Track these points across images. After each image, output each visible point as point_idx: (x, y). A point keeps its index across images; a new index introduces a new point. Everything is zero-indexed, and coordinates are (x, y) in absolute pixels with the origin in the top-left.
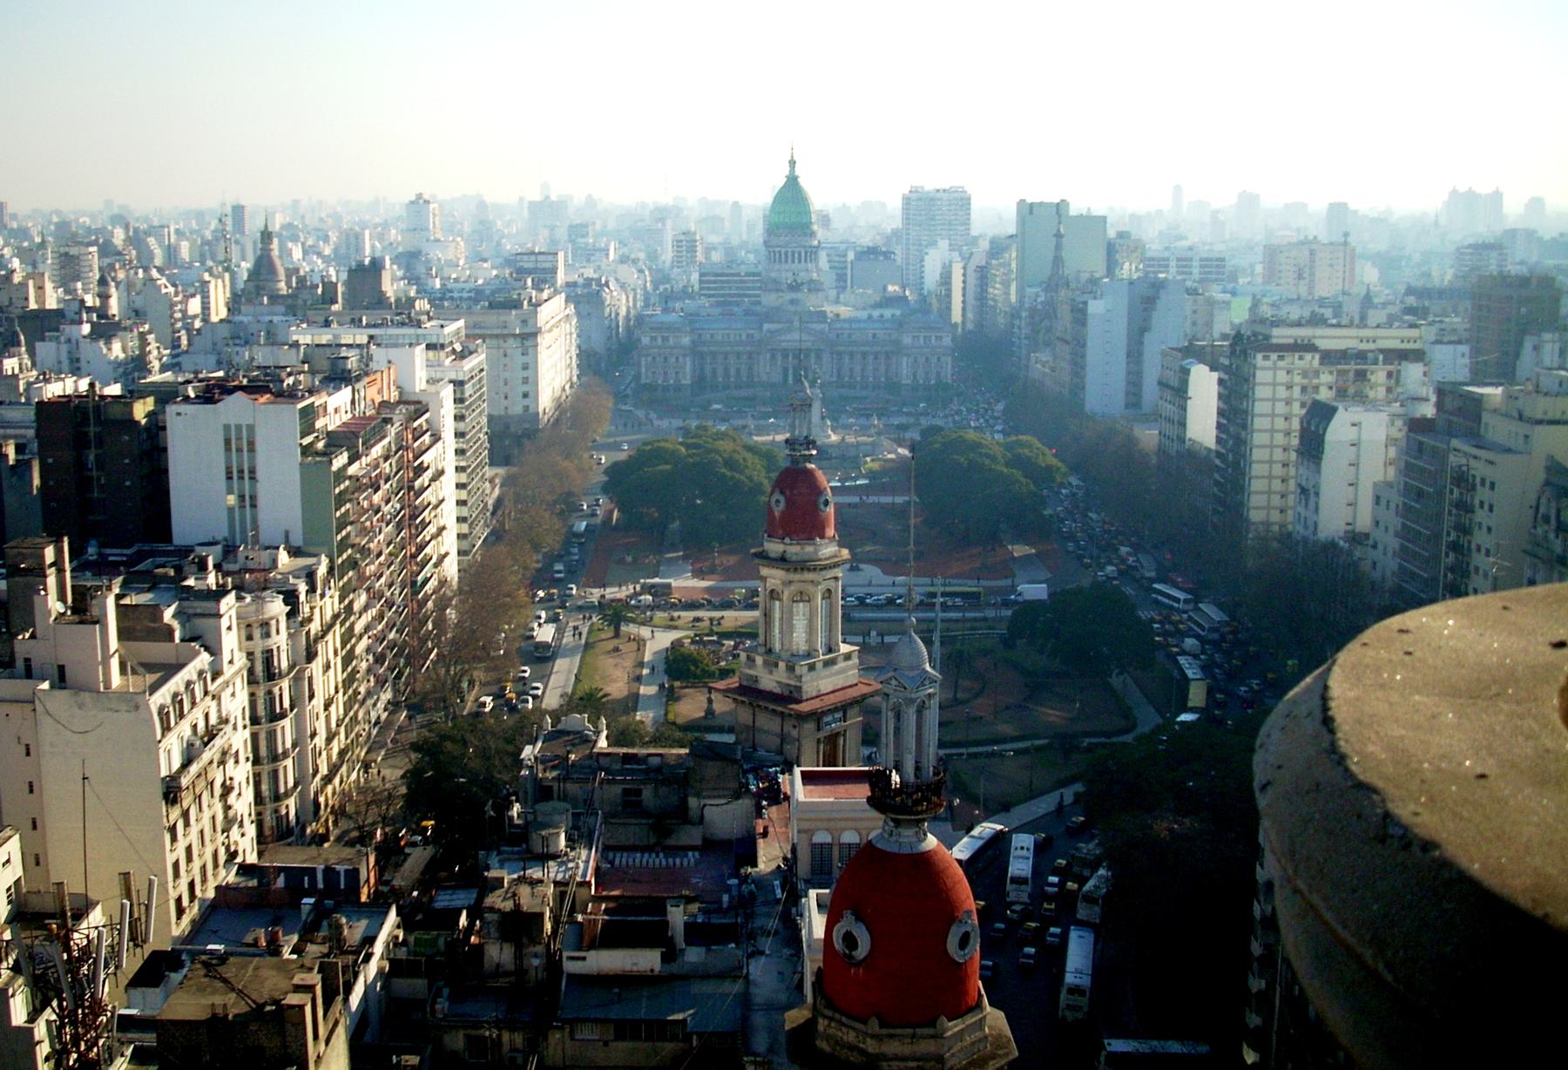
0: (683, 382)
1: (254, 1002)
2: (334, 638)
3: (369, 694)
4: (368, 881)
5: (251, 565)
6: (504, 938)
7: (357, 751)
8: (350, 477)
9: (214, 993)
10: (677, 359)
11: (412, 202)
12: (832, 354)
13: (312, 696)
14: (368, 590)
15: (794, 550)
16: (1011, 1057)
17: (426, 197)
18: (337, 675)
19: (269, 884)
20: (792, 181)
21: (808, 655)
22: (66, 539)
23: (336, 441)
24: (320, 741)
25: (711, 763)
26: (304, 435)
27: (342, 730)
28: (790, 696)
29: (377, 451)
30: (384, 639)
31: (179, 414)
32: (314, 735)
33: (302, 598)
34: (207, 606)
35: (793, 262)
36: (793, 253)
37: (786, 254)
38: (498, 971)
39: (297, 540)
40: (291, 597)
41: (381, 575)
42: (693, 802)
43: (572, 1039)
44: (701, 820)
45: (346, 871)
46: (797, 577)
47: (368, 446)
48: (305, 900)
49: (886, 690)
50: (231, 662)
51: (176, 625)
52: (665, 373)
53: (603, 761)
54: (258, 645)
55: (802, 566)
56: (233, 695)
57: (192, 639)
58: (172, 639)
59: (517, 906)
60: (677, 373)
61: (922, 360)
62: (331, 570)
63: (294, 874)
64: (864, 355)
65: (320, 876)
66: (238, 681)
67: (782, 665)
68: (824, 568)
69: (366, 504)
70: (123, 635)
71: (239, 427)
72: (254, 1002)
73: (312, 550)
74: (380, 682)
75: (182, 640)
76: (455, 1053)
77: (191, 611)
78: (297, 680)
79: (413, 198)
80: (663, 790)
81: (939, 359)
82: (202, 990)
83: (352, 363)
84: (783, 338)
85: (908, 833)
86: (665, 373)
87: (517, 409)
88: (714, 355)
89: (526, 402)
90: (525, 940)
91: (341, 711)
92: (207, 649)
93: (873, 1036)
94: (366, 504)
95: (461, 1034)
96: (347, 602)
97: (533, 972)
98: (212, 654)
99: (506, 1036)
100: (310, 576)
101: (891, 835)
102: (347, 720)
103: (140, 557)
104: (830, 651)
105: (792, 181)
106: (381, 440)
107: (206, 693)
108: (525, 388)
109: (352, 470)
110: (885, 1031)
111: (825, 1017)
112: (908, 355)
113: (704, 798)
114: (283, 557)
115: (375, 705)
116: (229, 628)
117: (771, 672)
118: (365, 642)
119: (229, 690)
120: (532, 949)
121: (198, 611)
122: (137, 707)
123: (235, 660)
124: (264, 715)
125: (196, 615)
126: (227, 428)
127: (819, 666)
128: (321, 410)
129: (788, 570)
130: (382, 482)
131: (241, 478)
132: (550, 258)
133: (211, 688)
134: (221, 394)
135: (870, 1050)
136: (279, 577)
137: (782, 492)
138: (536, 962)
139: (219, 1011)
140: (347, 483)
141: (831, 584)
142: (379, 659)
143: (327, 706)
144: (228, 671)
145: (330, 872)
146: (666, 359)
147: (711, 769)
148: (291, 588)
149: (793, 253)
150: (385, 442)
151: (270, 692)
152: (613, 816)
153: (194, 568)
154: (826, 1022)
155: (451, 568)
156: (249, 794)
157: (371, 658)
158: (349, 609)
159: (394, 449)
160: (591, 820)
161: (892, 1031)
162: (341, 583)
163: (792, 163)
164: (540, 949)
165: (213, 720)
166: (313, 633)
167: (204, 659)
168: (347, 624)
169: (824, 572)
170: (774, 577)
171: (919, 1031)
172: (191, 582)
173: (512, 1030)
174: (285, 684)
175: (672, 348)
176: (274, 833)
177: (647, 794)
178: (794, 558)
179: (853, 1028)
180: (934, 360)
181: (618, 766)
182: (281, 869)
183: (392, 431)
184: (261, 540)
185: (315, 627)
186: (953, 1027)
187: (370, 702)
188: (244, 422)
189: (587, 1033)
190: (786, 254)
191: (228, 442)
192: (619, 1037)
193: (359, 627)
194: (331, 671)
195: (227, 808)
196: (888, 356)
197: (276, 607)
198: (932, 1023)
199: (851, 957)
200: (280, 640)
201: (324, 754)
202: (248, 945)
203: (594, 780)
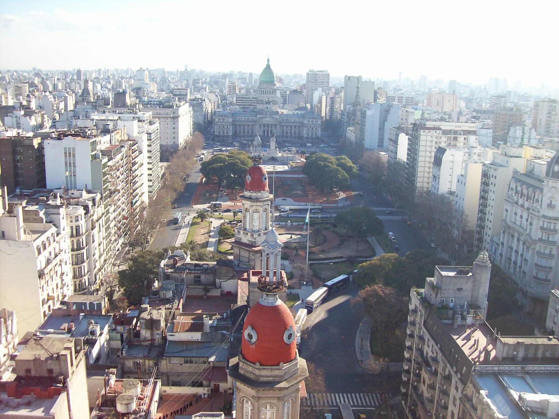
0: (230, 134)
1: (51, 353)
2: (102, 221)
3: (116, 240)
4: (105, 307)
5: (73, 196)
6: (147, 328)
7: (111, 260)
8: (109, 166)
9: (37, 349)
11: (138, 71)
12: (280, 126)
13: (93, 242)
14: (114, 205)
15: (254, 195)
16: (306, 376)
17: (144, 69)
18: (103, 234)
19: (70, 308)
20: (268, 67)
21: (259, 231)
22: (6, 187)
23: (105, 153)
24: (97, 257)
25: (224, 267)
26: (92, 151)
27: (105, 253)
28: (251, 245)
29: (119, 157)
30: (121, 221)
31: (49, 143)
32: (94, 255)
33: (90, 208)
34: (55, 211)
37: (266, 91)
38: (145, 340)
39: (90, 187)
40: (86, 208)
41: (120, 200)
42: (217, 281)
43: (170, 363)
44: (220, 287)
45: (97, 304)
46: (254, 204)
47: (115, 155)
48: (81, 314)
49: (264, 249)
50: (64, 230)
51: (44, 217)
52: (223, 131)
53: (188, 266)
54: (74, 224)
55: (257, 200)
56: (65, 241)
57: (50, 222)
58: (42, 222)
59: (151, 317)
60: (227, 131)
61: (310, 129)
62: (101, 198)
63: (79, 305)
65: (88, 305)
66: (67, 237)
67: (249, 234)
68: (264, 201)
69: (115, 175)
70: (25, 220)
71: (69, 148)
72: (51, 353)
73: (95, 191)
74: (120, 236)
75: (46, 222)
76: (129, 368)
77: (50, 213)
78: (88, 237)
79: (139, 69)
80: (208, 276)
81: (316, 128)
82: (32, 349)
83: (111, 127)
84: (264, 120)
85: (271, 299)
86: (223, 131)
87: (172, 143)
88: (240, 125)
89: (174, 140)
90: (154, 329)
91: (105, 248)
92: (55, 225)
93: (257, 369)
94: (115, 175)
95: (131, 361)
96: (107, 209)
97: (157, 340)
98: (57, 227)
99: (147, 361)
100: (94, 200)
101: (265, 299)
102: (107, 249)
103: (35, 193)
104: (266, 229)
105: (268, 67)
106: (120, 153)
107: (54, 241)
109: (109, 164)
110: (262, 367)
111: (242, 362)
112: (306, 127)
113: (221, 279)
114: (84, 193)
115: (117, 244)
116: (63, 218)
117: (246, 237)
118: (114, 223)
119: (63, 239)
120: (157, 332)
121: (52, 212)
122: (29, 246)
123: (65, 229)
124: (77, 248)
125: (51, 214)
126: (65, 148)
127: (262, 234)
128: (99, 143)
129: (252, 202)
130: (120, 168)
131: (70, 166)
132: (185, 91)
133: (57, 239)
134: (63, 137)
135: (257, 374)
136: (83, 200)
137: (250, 175)
138: (158, 336)
139: (37, 356)
140: (107, 168)
141: (267, 207)
142: (119, 229)
143: (99, 245)
144: (63, 233)
145: (91, 304)
147: (224, 269)
148: (86, 204)
150: (122, 154)
151: (78, 240)
152: (191, 285)
153: (53, 197)
154: (242, 364)
155: (145, 199)
156: (71, 275)
157: (116, 228)
158: (108, 212)
159: (125, 156)
160: (182, 287)
161: (264, 367)
162: (105, 203)
163: (268, 60)
164: (159, 332)
165: (57, 251)
166: (94, 220)
167: (54, 229)
168: (107, 217)
169: (264, 203)
170: (248, 204)
171: (274, 367)
172: (50, 202)
173: (149, 360)
174: (84, 237)
175: (226, 123)
176: (80, 289)
177: (203, 277)
178: (254, 198)
179: (251, 366)
180: (315, 129)
181: (193, 268)
182: (74, 303)
183: (124, 150)
184: (77, 187)
185: (95, 218)
186: (286, 366)
187: (115, 243)
188: (72, 146)
189: (175, 361)
190: (266, 91)
191: (66, 153)
192: (186, 362)
193: (111, 218)
194: (101, 232)
195: (62, 280)
197: (81, 211)
198: (278, 365)
199: (250, 342)
200: (82, 223)
201: (98, 261)
202: (62, 329)
203: (184, 272)
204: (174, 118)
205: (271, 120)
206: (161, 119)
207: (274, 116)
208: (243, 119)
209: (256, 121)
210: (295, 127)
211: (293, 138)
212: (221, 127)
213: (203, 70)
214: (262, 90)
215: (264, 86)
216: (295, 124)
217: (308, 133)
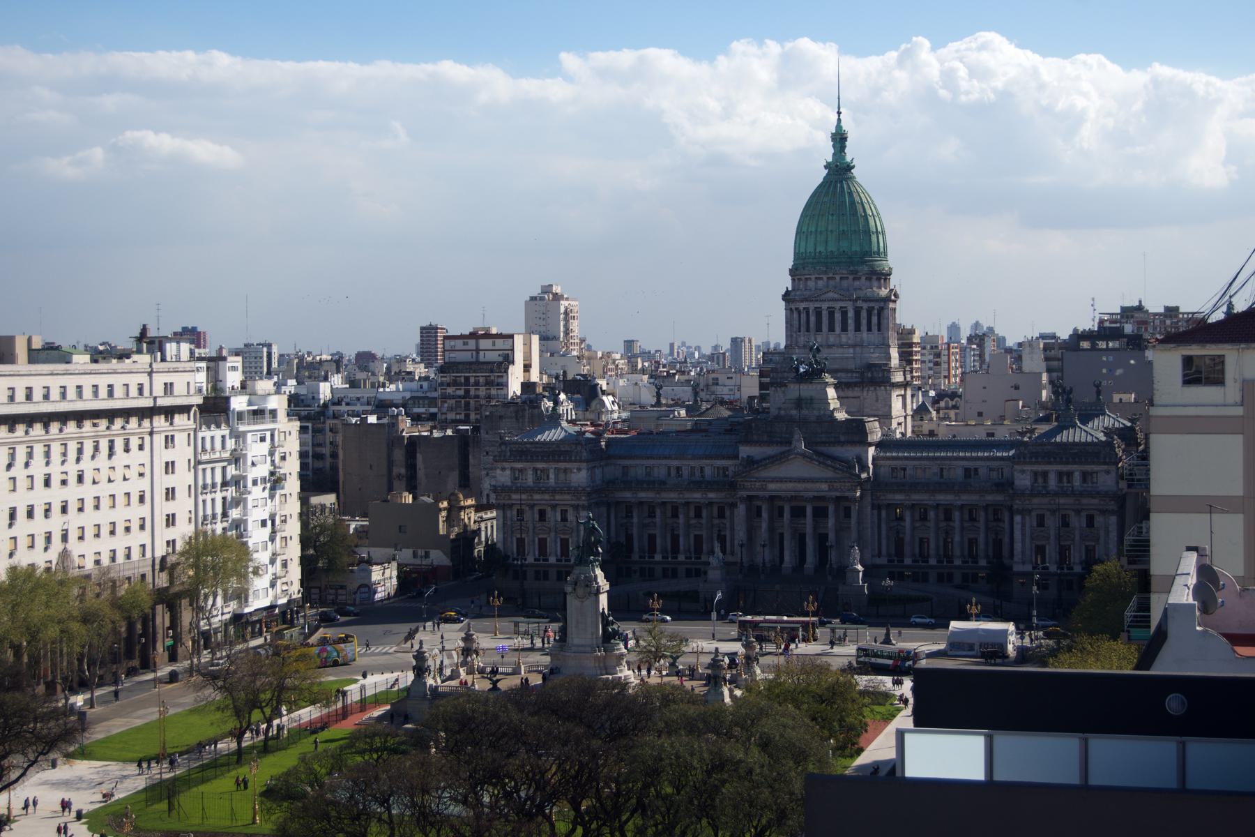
10: (564, 512)
11: (533, 299)
12: (877, 507)
17: (557, 289)
20: (839, 171)
35: (832, 329)
37: (818, 313)
52: (542, 543)
61: (1052, 523)
64: (948, 513)
79: (536, 291)
81: (1090, 521)
84: (774, 472)
88: (651, 509)
105: (839, 171)
132: (500, 343)
146: (542, 514)
163: (839, 139)
175: (554, 491)
180: (1078, 522)
190: (818, 313)
196: (995, 512)
205: (814, 471)
207: (838, 451)
208: (660, 471)
210: (971, 513)
211: (958, 579)
212: (530, 516)
214: (802, 306)
215: (811, 284)
216: (966, 498)
217: (1040, 550)
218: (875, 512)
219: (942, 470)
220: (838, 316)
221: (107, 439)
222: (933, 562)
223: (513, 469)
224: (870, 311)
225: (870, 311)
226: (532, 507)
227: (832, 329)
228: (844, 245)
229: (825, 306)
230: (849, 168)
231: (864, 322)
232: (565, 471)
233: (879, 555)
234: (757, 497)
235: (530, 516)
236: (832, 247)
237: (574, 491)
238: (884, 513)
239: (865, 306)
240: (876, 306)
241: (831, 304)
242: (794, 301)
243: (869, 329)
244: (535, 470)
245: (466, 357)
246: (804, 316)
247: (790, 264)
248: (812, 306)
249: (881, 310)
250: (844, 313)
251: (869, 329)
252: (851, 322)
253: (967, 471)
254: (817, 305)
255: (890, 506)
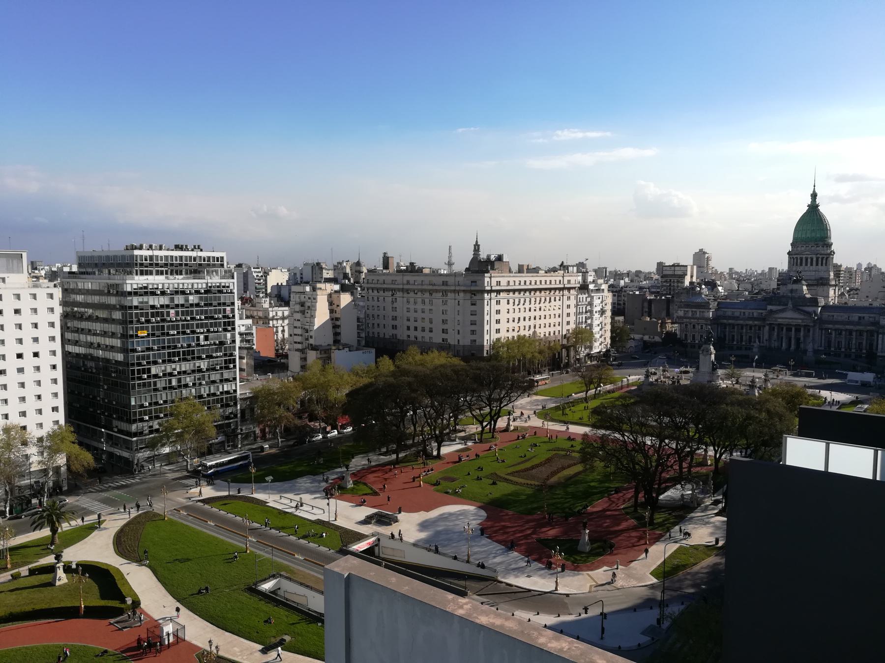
10: (702, 326)
12: (821, 329)
35: (806, 265)
36: (807, 259)
37: (801, 259)
52: (694, 336)
64: (850, 332)
88: (733, 326)
108: (473, 328)
132: (682, 268)
146: (694, 326)
149: (807, 259)
163: (814, 196)
190: (801, 259)
196: (871, 333)
204: (474, 293)
205: (796, 315)
206: (449, 294)
208: (737, 314)
209: (764, 319)
210: (860, 333)
212: (690, 327)
213: (873, 263)
215: (799, 249)
218: (820, 331)
219: (849, 317)
220: (809, 260)
221: (495, 300)
222: (843, 350)
223: (684, 311)
224: (822, 259)
225: (822, 259)
226: (690, 324)
227: (806, 265)
228: (813, 235)
229: (804, 256)
230: (818, 206)
231: (820, 262)
232: (703, 312)
233: (821, 346)
234: (773, 324)
235: (690, 327)
236: (809, 235)
237: (708, 319)
238: (823, 332)
239: (821, 256)
240: (825, 257)
241: (807, 256)
242: (792, 255)
243: (822, 265)
244: (692, 311)
245: (671, 273)
246: (795, 260)
247: (791, 242)
248: (799, 257)
249: (827, 258)
250: (812, 259)
251: (822, 265)
252: (814, 263)
253: (860, 318)
254: (801, 256)
255: (827, 329)
